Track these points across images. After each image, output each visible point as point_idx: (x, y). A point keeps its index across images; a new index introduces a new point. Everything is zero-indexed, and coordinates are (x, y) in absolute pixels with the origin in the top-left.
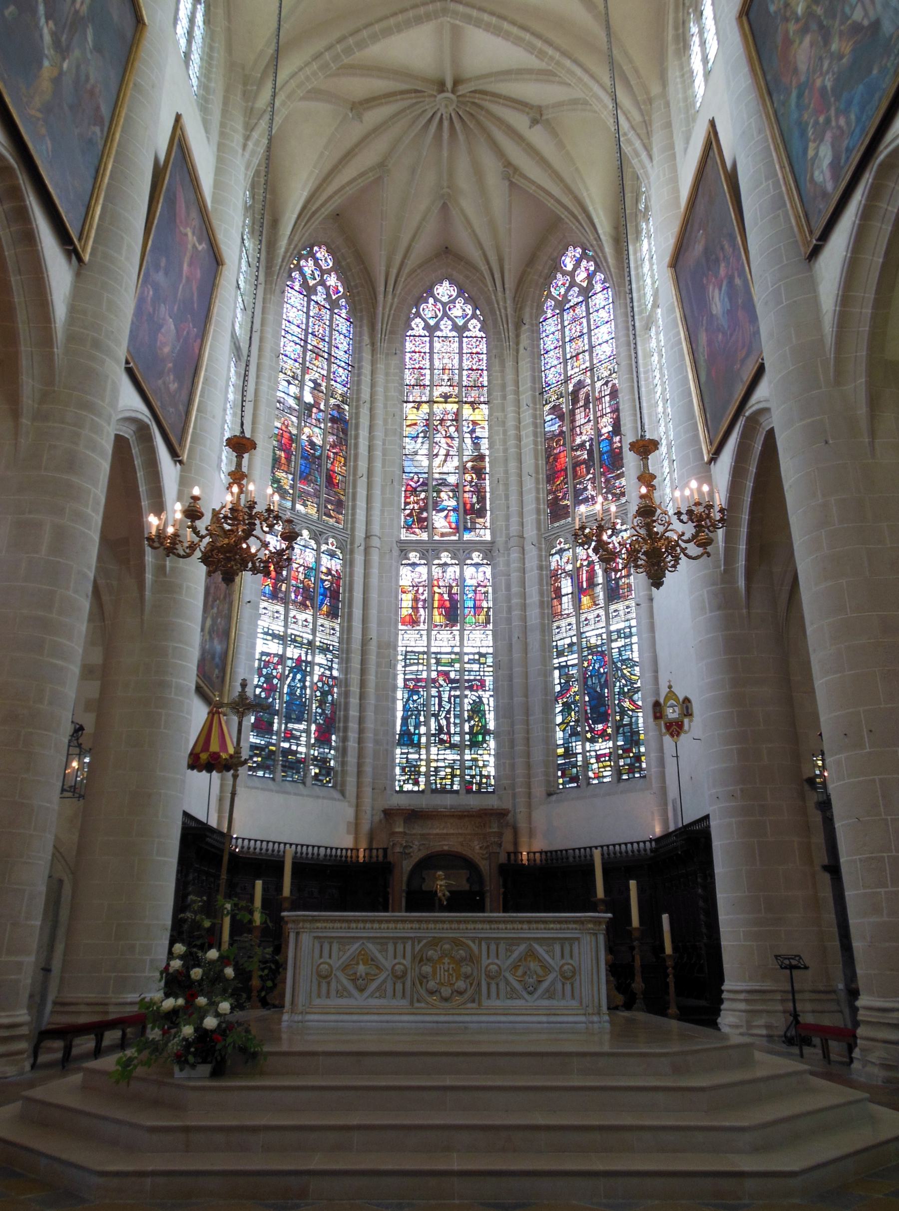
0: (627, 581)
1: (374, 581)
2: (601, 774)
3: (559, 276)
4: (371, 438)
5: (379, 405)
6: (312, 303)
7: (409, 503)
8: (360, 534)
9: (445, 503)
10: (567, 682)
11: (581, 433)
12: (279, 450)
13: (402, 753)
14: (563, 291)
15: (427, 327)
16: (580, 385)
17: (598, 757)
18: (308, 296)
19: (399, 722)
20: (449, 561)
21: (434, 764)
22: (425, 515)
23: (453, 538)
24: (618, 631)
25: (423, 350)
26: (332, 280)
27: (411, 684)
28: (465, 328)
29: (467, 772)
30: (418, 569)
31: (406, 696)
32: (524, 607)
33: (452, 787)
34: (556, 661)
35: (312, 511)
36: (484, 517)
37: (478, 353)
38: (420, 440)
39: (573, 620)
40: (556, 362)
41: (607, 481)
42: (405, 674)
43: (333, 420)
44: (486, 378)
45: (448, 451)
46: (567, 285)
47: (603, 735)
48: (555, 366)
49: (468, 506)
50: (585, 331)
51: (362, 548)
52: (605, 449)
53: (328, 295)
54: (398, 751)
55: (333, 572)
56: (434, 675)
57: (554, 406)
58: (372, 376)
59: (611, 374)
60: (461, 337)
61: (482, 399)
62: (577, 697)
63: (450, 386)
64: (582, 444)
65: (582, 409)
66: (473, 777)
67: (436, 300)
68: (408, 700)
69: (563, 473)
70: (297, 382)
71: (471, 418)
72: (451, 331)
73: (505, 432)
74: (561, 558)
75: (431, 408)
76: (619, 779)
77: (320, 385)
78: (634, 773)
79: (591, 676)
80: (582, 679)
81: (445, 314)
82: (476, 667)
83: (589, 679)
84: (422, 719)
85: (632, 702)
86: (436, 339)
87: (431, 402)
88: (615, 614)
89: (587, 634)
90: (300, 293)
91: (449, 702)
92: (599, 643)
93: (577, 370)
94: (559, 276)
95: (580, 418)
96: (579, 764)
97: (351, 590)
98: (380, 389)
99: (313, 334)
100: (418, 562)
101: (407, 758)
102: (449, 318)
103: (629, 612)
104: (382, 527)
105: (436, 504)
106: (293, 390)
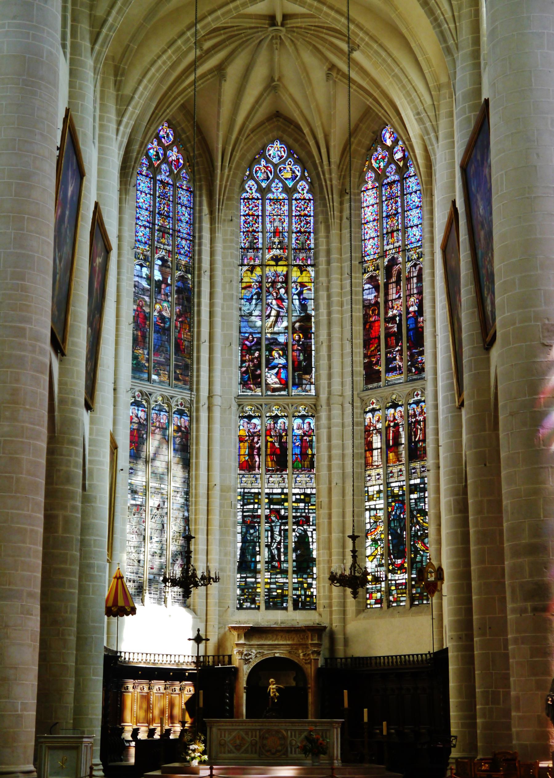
0: (424, 445)
2: (398, 599)
3: (379, 149)
4: (212, 305)
5: (219, 273)
8: (204, 393)
9: (276, 361)
10: (375, 522)
11: (393, 308)
12: (136, 330)
13: (241, 578)
14: (382, 164)
15: (260, 189)
16: (393, 262)
17: (397, 585)
18: (154, 179)
19: (239, 552)
20: (280, 415)
21: (268, 586)
22: (259, 372)
23: (283, 393)
24: (415, 485)
26: (173, 155)
27: (248, 520)
28: (294, 190)
29: (294, 592)
30: (254, 421)
31: (244, 530)
32: (343, 455)
33: (283, 605)
34: (367, 504)
35: (165, 379)
36: (310, 373)
37: (306, 215)
38: (254, 302)
39: (381, 471)
40: (373, 234)
41: (412, 356)
42: (243, 512)
43: (179, 291)
44: (312, 241)
46: (386, 160)
47: (401, 567)
48: (373, 238)
49: (296, 363)
50: (399, 210)
51: (206, 406)
52: (411, 326)
53: (171, 171)
54: (239, 576)
55: (183, 429)
56: (267, 512)
57: (372, 276)
58: (211, 244)
59: (418, 258)
60: (290, 200)
61: (309, 263)
62: (383, 536)
63: (280, 249)
65: (394, 285)
66: (299, 596)
67: (268, 161)
68: (246, 533)
69: (377, 341)
70: (148, 264)
71: (299, 280)
72: (280, 193)
73: (329, 297)
74: (373, 417)
75: (262, 270)
76: (412, 605)
77: (167, 261)
78: (423, 600)
79: (393, 520)
80: (387, 521)
82: (302, 505)
83: (392, 522)
84: (258, 549)
85: (424, 544)
86: (268, 201)
87: (262, 265)
88: (413, 471)
89: (392, 485)
90: (147, 176)
92: (401, 493)
93: (391, 246)
94: (379, 149)
95: (392, 291)
96: (383, 589)
97: (197, 444)
98: (218, 258)
100: (253, 415)
101: (246, 581)
103: (424, 471)
104: (222, 386)
105: (268, 362)
106: (145, 271)
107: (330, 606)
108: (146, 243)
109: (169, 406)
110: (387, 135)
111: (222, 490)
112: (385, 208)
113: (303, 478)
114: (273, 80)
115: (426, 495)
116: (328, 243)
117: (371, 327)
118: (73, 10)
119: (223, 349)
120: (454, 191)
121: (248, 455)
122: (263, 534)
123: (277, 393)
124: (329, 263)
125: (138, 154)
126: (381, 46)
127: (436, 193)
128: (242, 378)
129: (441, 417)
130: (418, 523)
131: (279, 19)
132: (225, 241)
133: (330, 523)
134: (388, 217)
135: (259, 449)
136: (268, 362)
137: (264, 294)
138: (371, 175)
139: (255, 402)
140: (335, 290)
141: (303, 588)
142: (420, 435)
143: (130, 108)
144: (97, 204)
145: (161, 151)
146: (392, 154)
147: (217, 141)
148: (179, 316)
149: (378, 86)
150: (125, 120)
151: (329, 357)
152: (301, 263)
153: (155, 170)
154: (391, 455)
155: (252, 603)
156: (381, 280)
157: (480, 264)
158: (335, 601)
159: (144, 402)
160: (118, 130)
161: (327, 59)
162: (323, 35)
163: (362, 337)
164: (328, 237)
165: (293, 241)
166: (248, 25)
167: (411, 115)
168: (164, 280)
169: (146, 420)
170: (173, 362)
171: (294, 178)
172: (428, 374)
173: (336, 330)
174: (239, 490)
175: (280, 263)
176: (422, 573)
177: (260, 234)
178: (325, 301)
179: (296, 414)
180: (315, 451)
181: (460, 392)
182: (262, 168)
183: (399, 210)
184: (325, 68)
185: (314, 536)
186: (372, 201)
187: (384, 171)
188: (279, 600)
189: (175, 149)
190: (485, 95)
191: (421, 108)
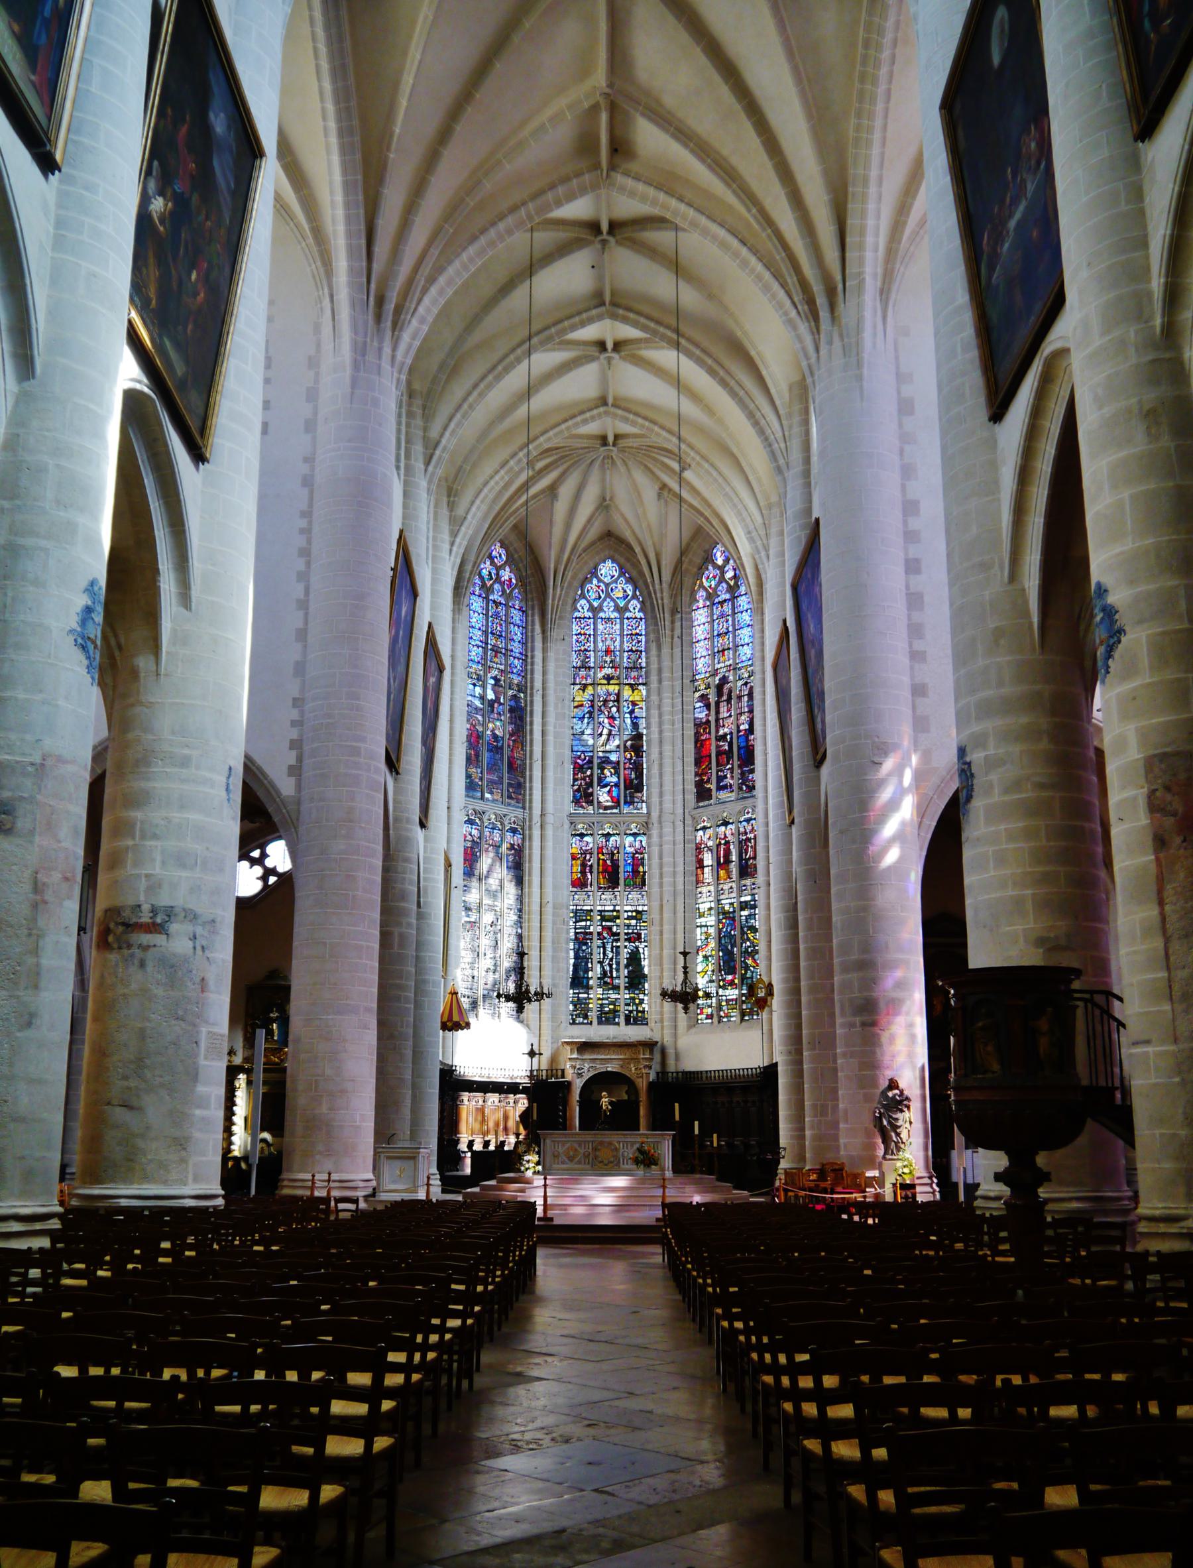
1: (549, 852)
3: (710, 568)
4: (544, 724)
5: (551, 692)
6: (491, 604)
7: (577, 780)
8: (537, 812)
9: (608, 780)
10: (707, 939)
11: (724, 726)
14: (713, 584)
15: (592, 609)
16: (724, 680)
17: (727, 1001)
18: (487, 598)
19: (571, 968)
21: (600, 1002)
22: (591, 790)
23: (615, 811)
24: (746, 902)
25: (588, 632)
26: (506, 574)
28: (626, 609)
29: (626, 1008)
30: (586, 839)
31: (577, 946)
34: (698, 921)
35: (498, 797)
36: (641, 791)
37: (637, 634)
38: (586, 720)
39: (712, 888)
41: (743, 774)
42: (576, 929)
43: (511, 710)
44: (644, 660)
45: (610, 731)
46: (717, 579)
47: (732, 983)
50: (730, 629)
51: (539, 824)
52: (743, 744)
53: (503, 591)
54: (571, 991)
56: (599, 929)
59: (749, 677)
64: (724, 737)
65: (725, 703)
66: (631, 1012)
67: (599, 581)
68: (578, 950)
73: (660, 716)
76: (742, 1020)
77: (499, 680)
79: (724, 936)
81: (608, 595)
82: (633, 922)
84: (590, 965)
85: (754, 961)
89: (723, 902)
90: (480, 596)
91: (612, 951)
92: (731, 910)
93: (722, 665)
94: (710, 568)
97: (530, 861)
98: (551, 677)
99: (492, 633)
102: (613, 600)
105: (600, 780)
106: (478, 690)
107: (662, 1021)
108: (479, 662)
109: (502, 824)
110: (718, 554)
111: (554, 907)
112: (716, 627)
113: (634, 895)
114: (604, 499)
115: (757, 912)
116: (659, 662)
117: (702, 745)
118: (407, 433)
119: (555, 767)
120: (784, 610)
121: (581, 872)
122: (595, 951)
123: (609, 811)
124: (660, 681)
125: (471, 573)
126: (712, 465)
127: (767, 611)
128: (574, 796)
129: (771, 835)
130: (748, 939)
131: (611, 439)
132: (557, 660)
133: (661, 940)
134: (719, 635)
135: (591, 866)
136: (600, 780)
137: (596, 713)
138: (702, 594)
139: (587, 820)
140: (667, 708)
141: (634, 1003)
142: (750, 853)
143: (463, 529)
144: (430, 624)
145: (494, 572)
146: (723, 573)
147: (550, 561)
148: (511, 735)
149: (709, 506)
150: (458, 540)
151: (661, 775)
152: (632, 682)
153: (488, 590)
154: (722, 873)
155: (584, 1019)
156: (712, 699)
157: (810, 681)
158: (666, 1016)
159: (477, 821)
160: (451, 551)
161: (658, 478)
162: (654, 455)
163: (693, 755)
164: (659, 656)
165: (625, 660)
166: (579, 446)
167: (742, 534)
168: (497, 700)
169: (480, 838)
170: (506, 781)
171: (626, 597)
172: (758, 792)
173: (667, 748)
174: (571, 907)
175: (611, 682)
176: (752, 989)
177: (592, 653)
178: (657, 719)
179: (628, 832)
180: (646, 869)
181: (790, 811)
182: (593, 586)
183: (730, 629)
184: (657, 487)
185: (646, 953)
186: (702, 619)
187: (715, 590)
188: (611, 1016)
189: (507, 569)
190: (815, 515)
191: (751, 527)
